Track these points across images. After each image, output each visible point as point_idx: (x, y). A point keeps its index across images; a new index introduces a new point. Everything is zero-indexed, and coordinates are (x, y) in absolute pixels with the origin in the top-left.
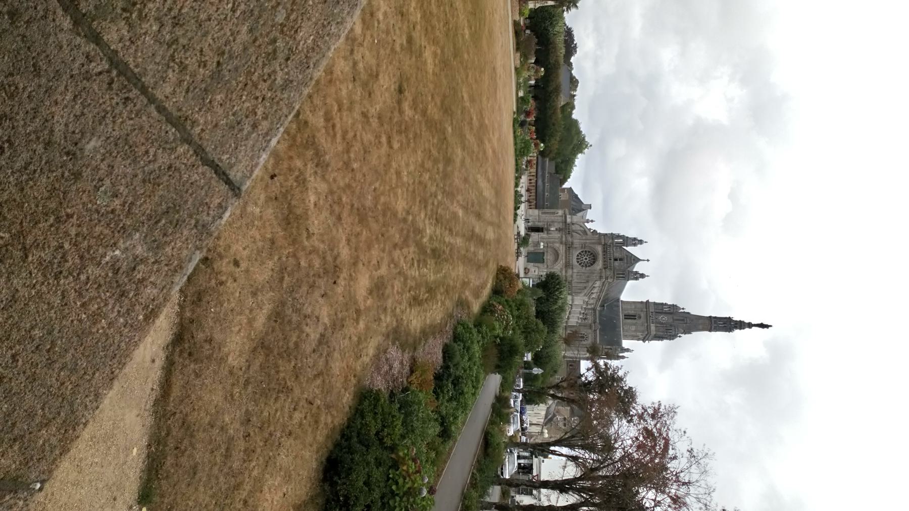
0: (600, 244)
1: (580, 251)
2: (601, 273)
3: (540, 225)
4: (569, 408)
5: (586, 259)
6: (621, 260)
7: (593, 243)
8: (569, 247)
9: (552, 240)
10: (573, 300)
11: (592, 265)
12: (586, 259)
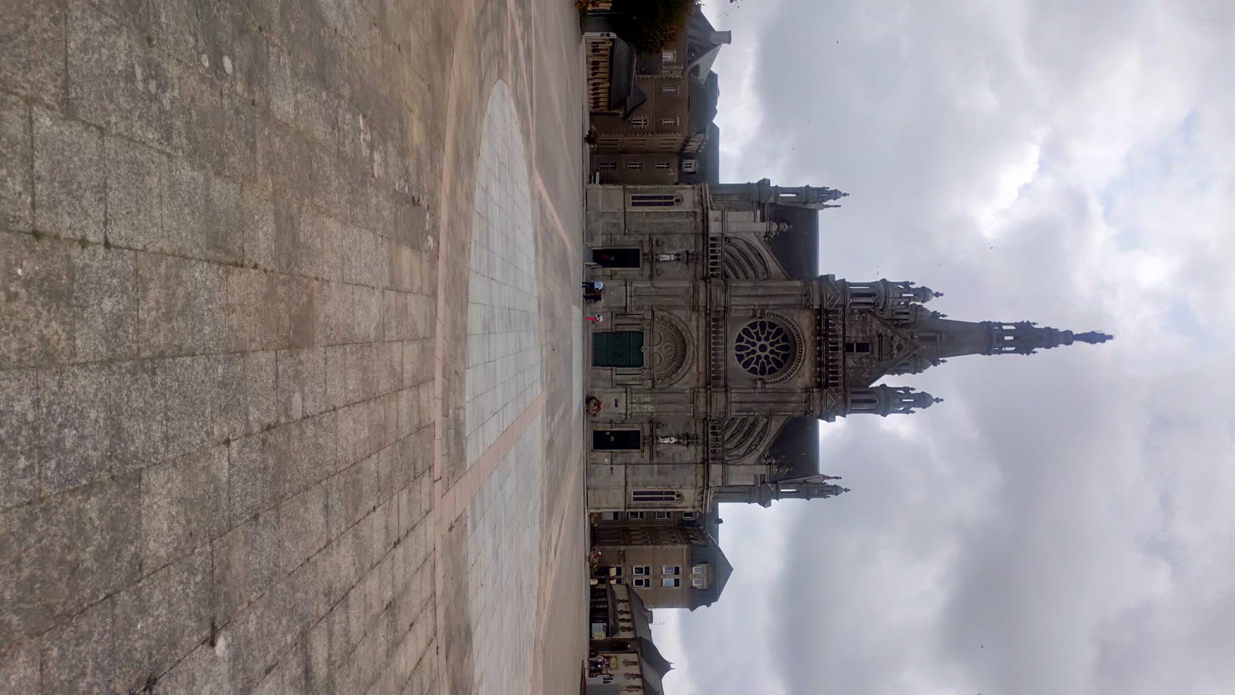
0: (807, 307)
1: (745, 326)
3: (629, 242)
4: (686, 547)
5: (763, 348)
6: (862, 347)
8: (716, 319)
9: (666, 301)
10: (725, 475)
11: (779, 365)
12: (763, 348)
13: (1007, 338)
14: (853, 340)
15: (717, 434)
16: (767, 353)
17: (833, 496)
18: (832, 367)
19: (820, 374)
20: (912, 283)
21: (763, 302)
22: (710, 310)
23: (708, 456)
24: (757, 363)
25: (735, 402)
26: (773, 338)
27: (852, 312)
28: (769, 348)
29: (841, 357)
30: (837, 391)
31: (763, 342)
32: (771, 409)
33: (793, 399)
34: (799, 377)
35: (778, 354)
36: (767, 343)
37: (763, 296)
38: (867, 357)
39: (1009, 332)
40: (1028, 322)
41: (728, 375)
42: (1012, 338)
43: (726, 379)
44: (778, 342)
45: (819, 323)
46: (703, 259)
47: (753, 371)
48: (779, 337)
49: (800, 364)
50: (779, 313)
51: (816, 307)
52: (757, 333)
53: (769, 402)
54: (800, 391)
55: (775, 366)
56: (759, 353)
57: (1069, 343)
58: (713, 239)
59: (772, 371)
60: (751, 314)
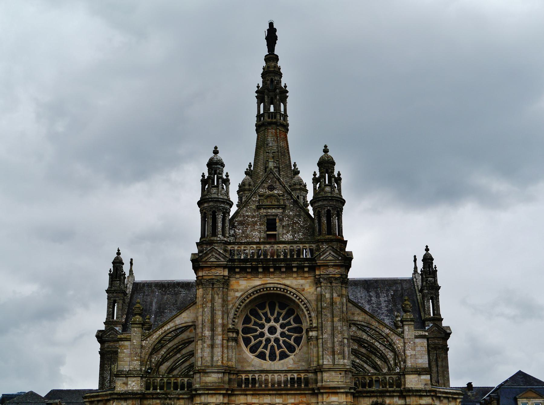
0: (226, 283)
1: (246, 351)
2: (330, 280)
5: (272, 330)
6: (271, 224)
7: (225, 302)
10: (419, 372)
12: (272, 330)
13: (272, 109)
14: (263, 235)
15: (371, 381)
16: (277, 326)
17: (435, 263)
18: (292, 256)
19: (301, 269)
20: (203, 176)
21: (220, 329)
22: (227, 390)
23: (397, 392)
24: (289, 337)
25: (334, 359)
26: (261, 319)
27: (233, 236)
28: (272, 323)
29: (281, 246)
30: (318, 249)
31: (266, 330)
32: (340, 320)
33: (328, 296)
34: (303, 290)
35: (279, 314)
36: (267, 326)
37: (213, 330)
38: (281, 220)
39: (266, 109)
40: (256, 92)
41: (304, 368)
42: (272, 106)
43: (307, 371)
44: (265, 314)
45: (243, 270)
46: (170, 399)
47: (298, 341)
48: (260, 313)
49: (289, 289)
50: (233, 311)
51: (226, 273)
52: (255, 337)
53: (333, 321)
54: (319, 289)
55: (292, 317)
56: (278, 335)
57: (276, 58)
58: (148, 388)
59: (298, 320)
60: (234, 344)
